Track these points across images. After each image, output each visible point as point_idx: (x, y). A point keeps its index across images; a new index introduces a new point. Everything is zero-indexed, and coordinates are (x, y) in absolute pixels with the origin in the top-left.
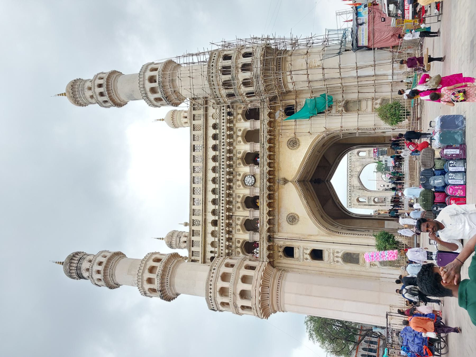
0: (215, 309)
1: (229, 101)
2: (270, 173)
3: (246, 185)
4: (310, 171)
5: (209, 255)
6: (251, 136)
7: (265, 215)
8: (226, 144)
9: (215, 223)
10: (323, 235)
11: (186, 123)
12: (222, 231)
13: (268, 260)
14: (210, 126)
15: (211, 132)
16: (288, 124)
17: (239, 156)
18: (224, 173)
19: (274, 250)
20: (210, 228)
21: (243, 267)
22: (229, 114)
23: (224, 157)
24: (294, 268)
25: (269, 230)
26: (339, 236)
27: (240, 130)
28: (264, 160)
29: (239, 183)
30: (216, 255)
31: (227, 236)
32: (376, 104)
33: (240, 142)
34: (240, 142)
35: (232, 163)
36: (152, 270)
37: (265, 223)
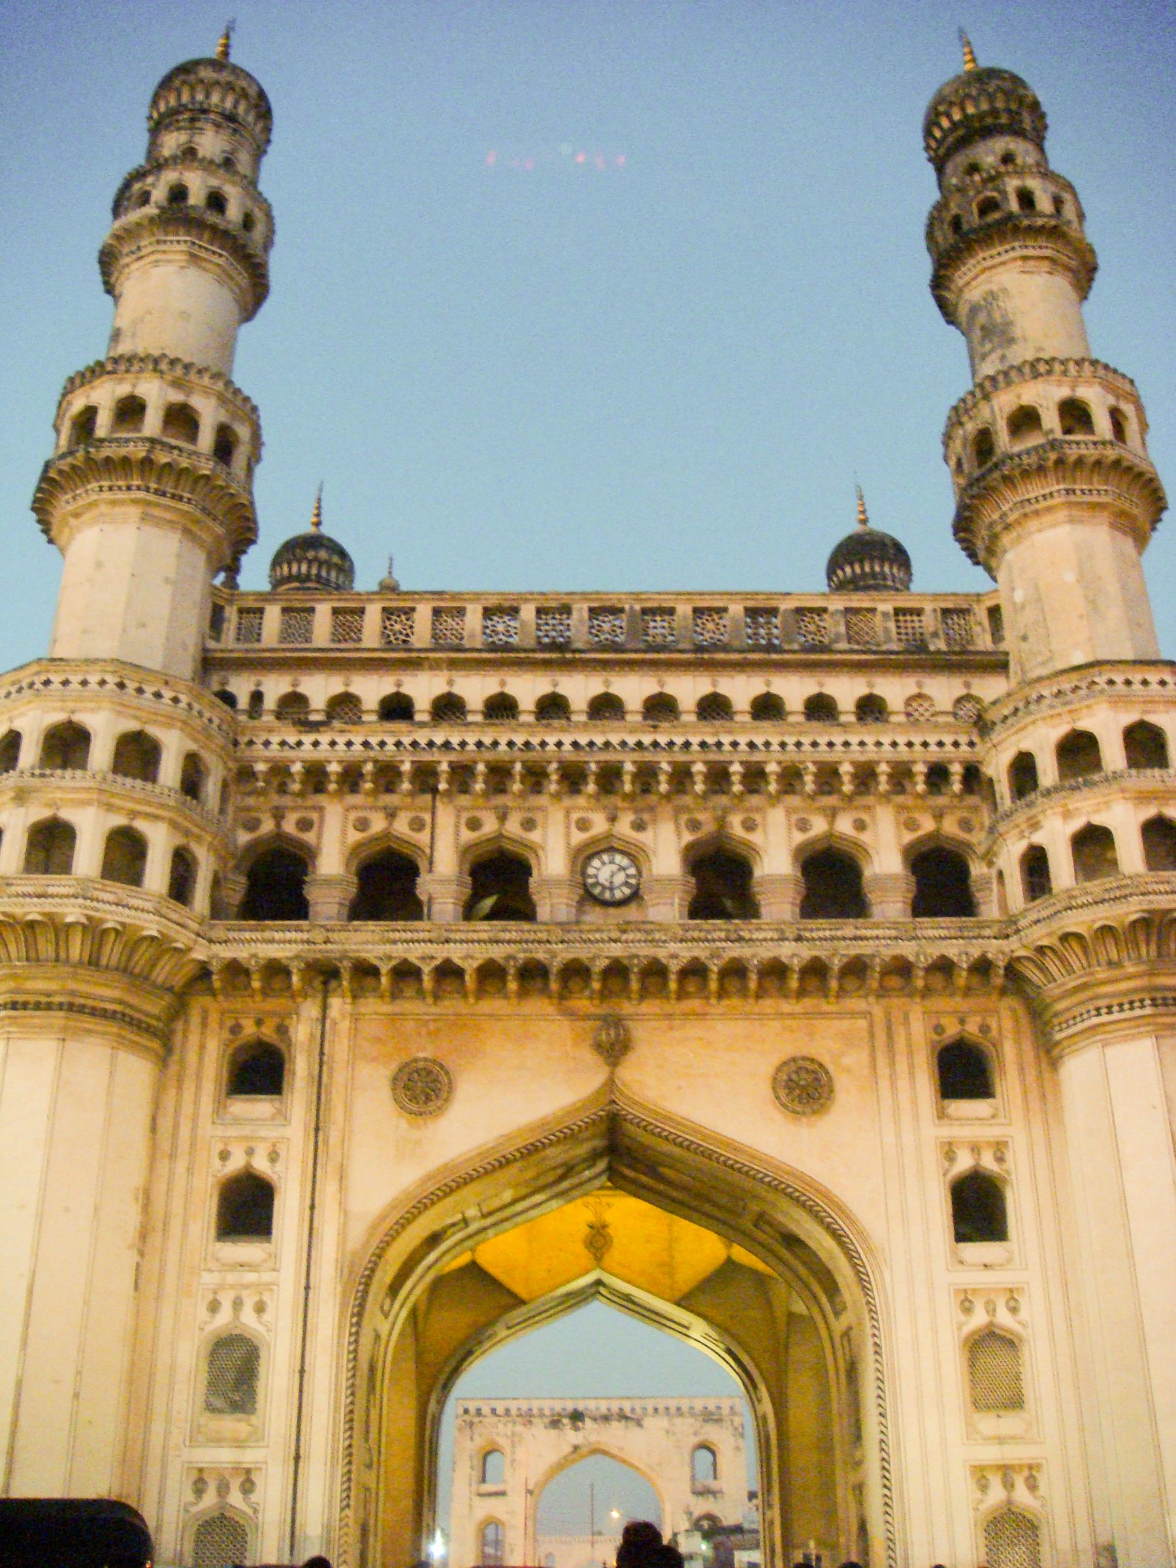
1: (997, 767)
2: (655, 971)
3: (590, 858)
4: (661, 1178)
5: (241, 686)
6: (832, 880)
7: (441, 952)
9: (397, 709)
10: (343, 1233)
12: (358, 740)
13: (215, 966)
14: (870, 685)
15: (846, 691)
19: (265, 992)
20: (372, 689)
21: (180, 840)
22: (938, 774)
24: (179, 1088)
25: (365, 971)
26: (342, 1313)
27: (860, 826)
28: (716, 943)
29: (599, 824)
31: (334, 768)
32: (1009, 1485)
33: (803, 826)
34: (803, 826)
35: (699, 787)
36: (181, 419)
37: (399, 951)
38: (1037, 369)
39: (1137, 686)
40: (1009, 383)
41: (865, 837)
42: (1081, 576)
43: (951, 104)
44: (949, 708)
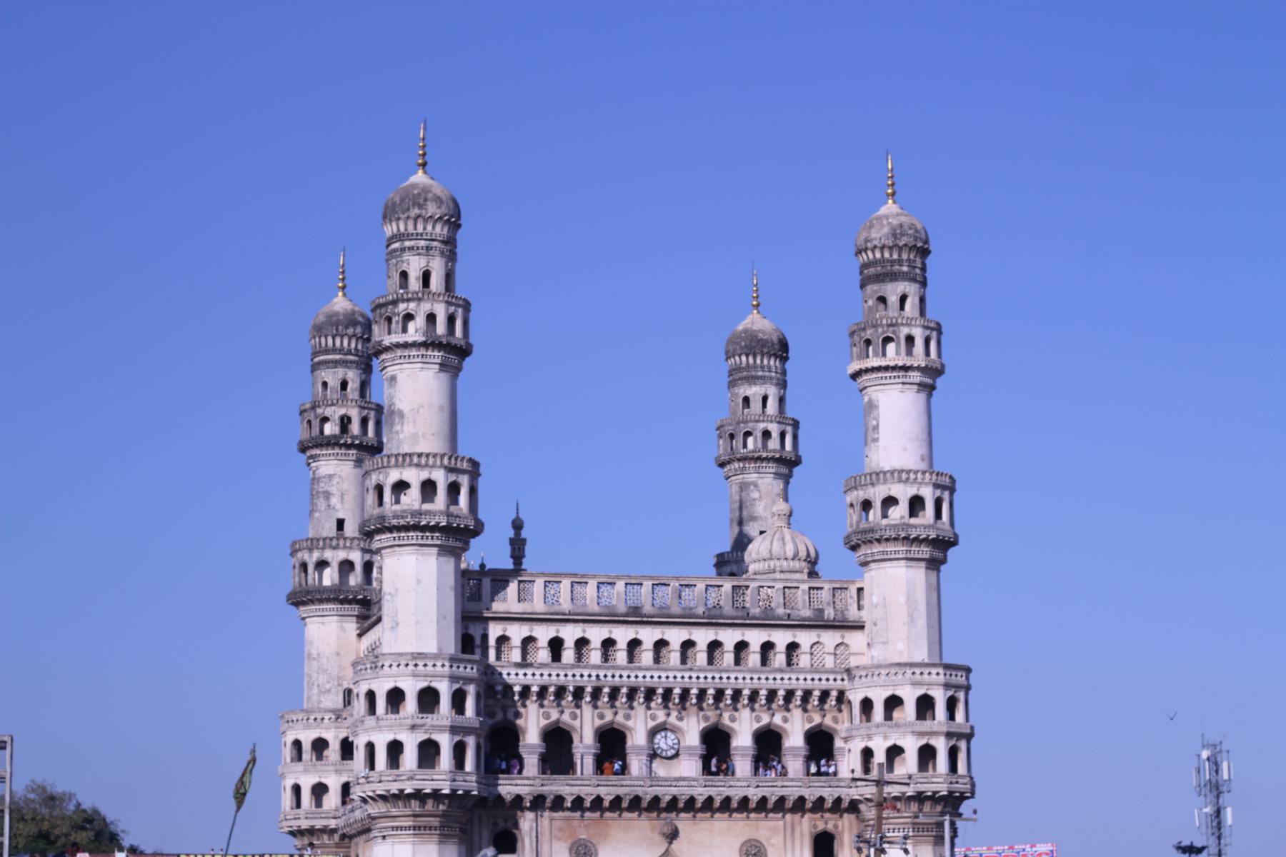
0: (381, 673)
1: (856, 698)
6: (768, 745)
8: (755, 686)
9: (556, 646)
11: (746, 400)
13: (491, 799)
16: (798, 841)
17: (726, 720)
18: (687, 680)
20: (544, 634)
23: (725, 680)
27: (785, 720)
29: (661, 716)
30: (478, 651)
33: (758, 719)
34: (758, 719)
37: (576, 790)
38: (901, 475)
39: (926, 676)
40: (885, 481)
41: (787, 726)
42: (908, 598)
43: (875, 247)
44: (832, 650)
